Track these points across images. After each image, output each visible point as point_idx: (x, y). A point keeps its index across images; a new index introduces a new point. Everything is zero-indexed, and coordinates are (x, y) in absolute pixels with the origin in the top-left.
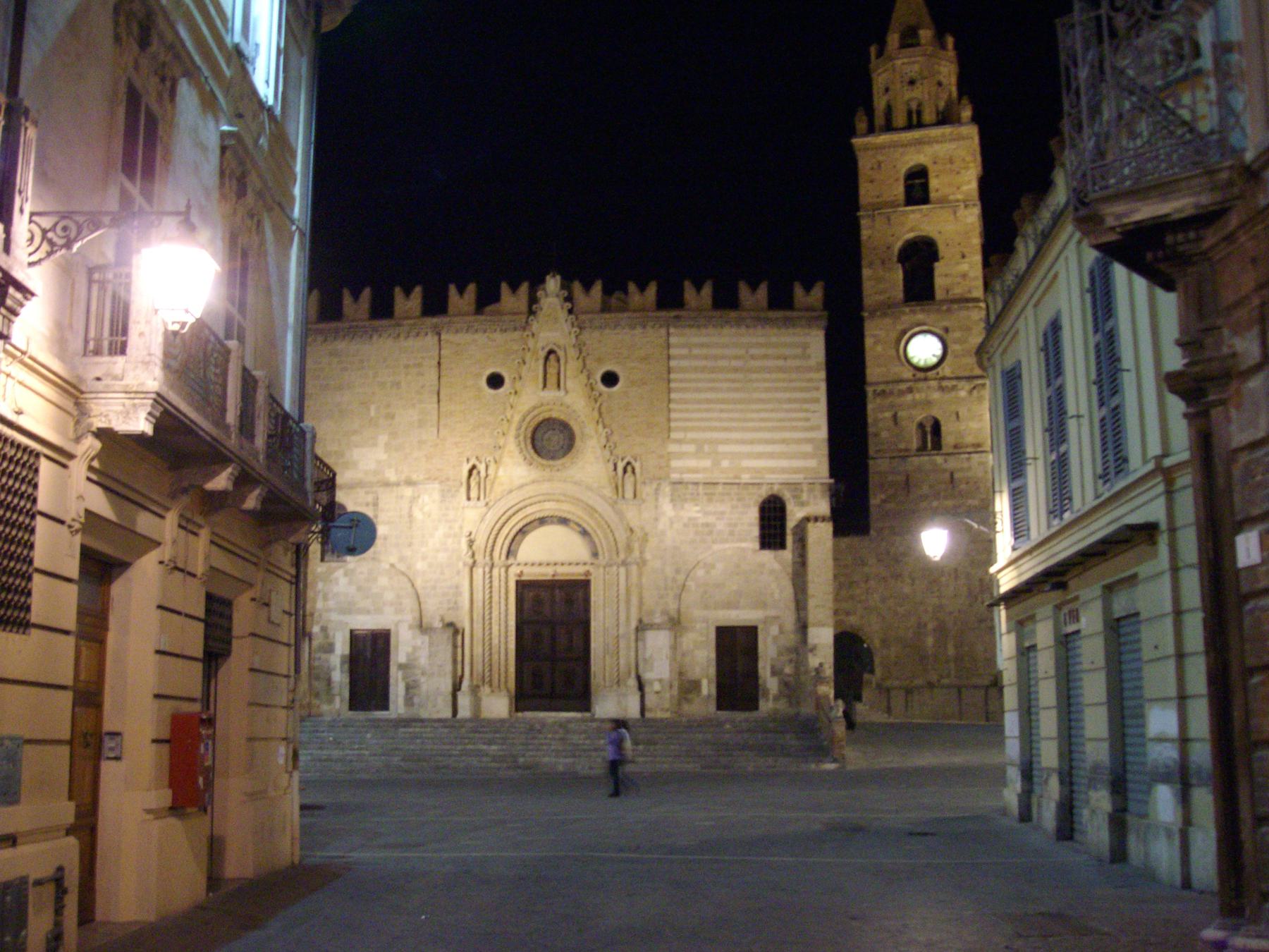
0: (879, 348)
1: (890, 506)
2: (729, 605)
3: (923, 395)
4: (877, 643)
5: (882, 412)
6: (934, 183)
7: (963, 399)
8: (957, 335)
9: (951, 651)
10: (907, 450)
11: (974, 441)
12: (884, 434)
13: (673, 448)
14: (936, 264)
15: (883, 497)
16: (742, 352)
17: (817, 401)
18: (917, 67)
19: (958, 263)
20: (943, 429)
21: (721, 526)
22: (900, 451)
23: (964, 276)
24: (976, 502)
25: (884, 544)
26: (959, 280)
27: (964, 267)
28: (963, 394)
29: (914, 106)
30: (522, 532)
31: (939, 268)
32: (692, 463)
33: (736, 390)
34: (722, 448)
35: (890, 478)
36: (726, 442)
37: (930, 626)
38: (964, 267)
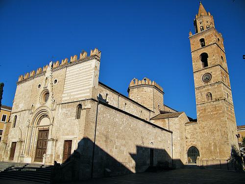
1: (201, 115)
2: (68, 135)
4: (200, 149)
9: (218, 151)
13: (63, 95)
16: (78, 69)
17: (92, 77)
21: (69, 114)
24: (221, 112)
29: (202, 28)
30: (40, 119)
32: (66, 98)
33: (77, 79)
34: (72, 94)
36: (72, 92)
37: (212, 144)
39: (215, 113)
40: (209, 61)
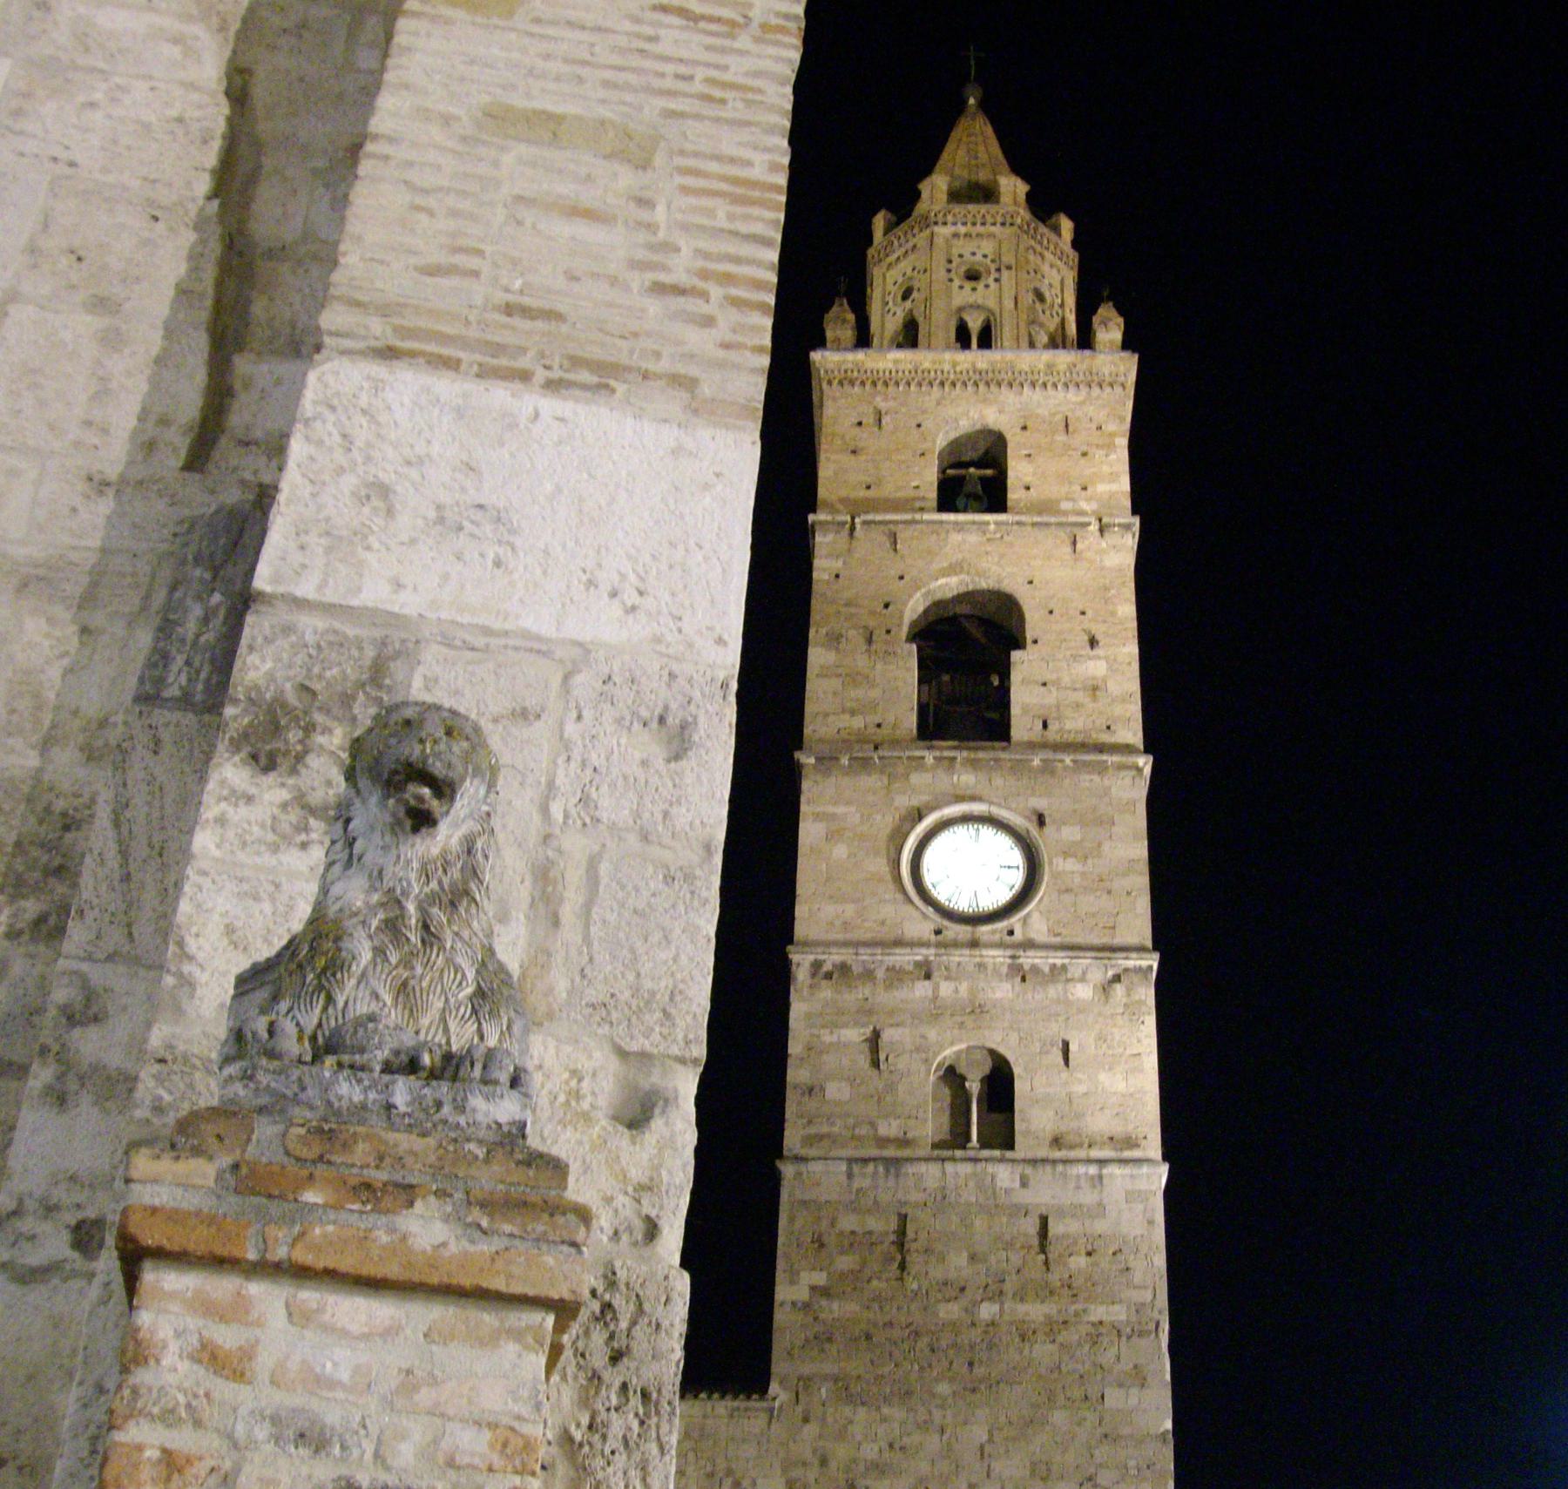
0: (840, 851)
1: (834, 1309)
3: (964, 987)
5: (834, 1026)
6: (1018, 471)
7: (1083, 1008)
8: (1071, 833)
10: (904, 1142)
11: (1118, 1129)
12: (836, 1091)
14: (1016, 655)
15: (820, 1279)
18: (988, 247)
19: (1075, 658)
20: (1020, 1087)
22: (883, 1142)
23: (1094, 689)
24: (1118, 1313)
25: (811, 1430)
26: (1080, 696)
27: (1096, 668)
28: (1083, 992)
31: (1023, 664)
35: (848, 1223)
38: (1096, 668)
39: (1035, 1311)
40: (1032, 683)
